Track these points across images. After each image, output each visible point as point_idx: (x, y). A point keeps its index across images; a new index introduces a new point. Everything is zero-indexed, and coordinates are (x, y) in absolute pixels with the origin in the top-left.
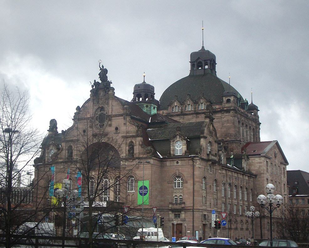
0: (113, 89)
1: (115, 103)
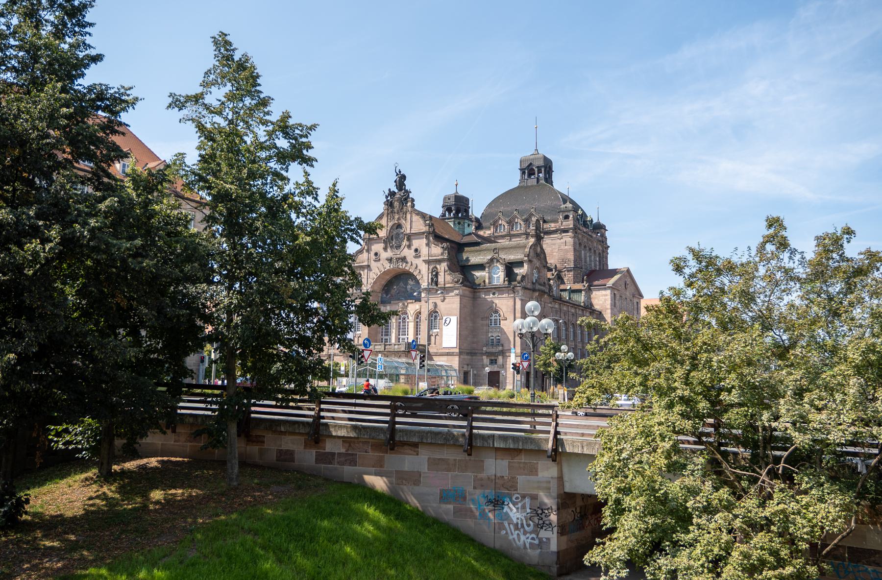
0: (413, 200)
1: (415, 218)
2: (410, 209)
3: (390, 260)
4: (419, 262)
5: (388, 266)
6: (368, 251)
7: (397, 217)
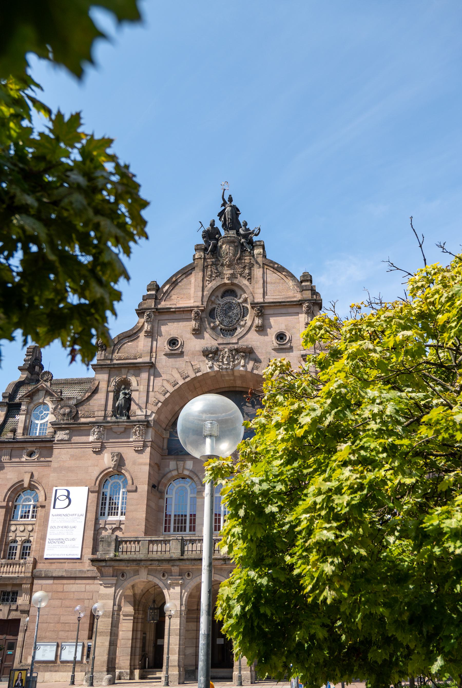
2: (260, 260)
3: (211, 354)
6: (152, 335)
7: (227, 272)
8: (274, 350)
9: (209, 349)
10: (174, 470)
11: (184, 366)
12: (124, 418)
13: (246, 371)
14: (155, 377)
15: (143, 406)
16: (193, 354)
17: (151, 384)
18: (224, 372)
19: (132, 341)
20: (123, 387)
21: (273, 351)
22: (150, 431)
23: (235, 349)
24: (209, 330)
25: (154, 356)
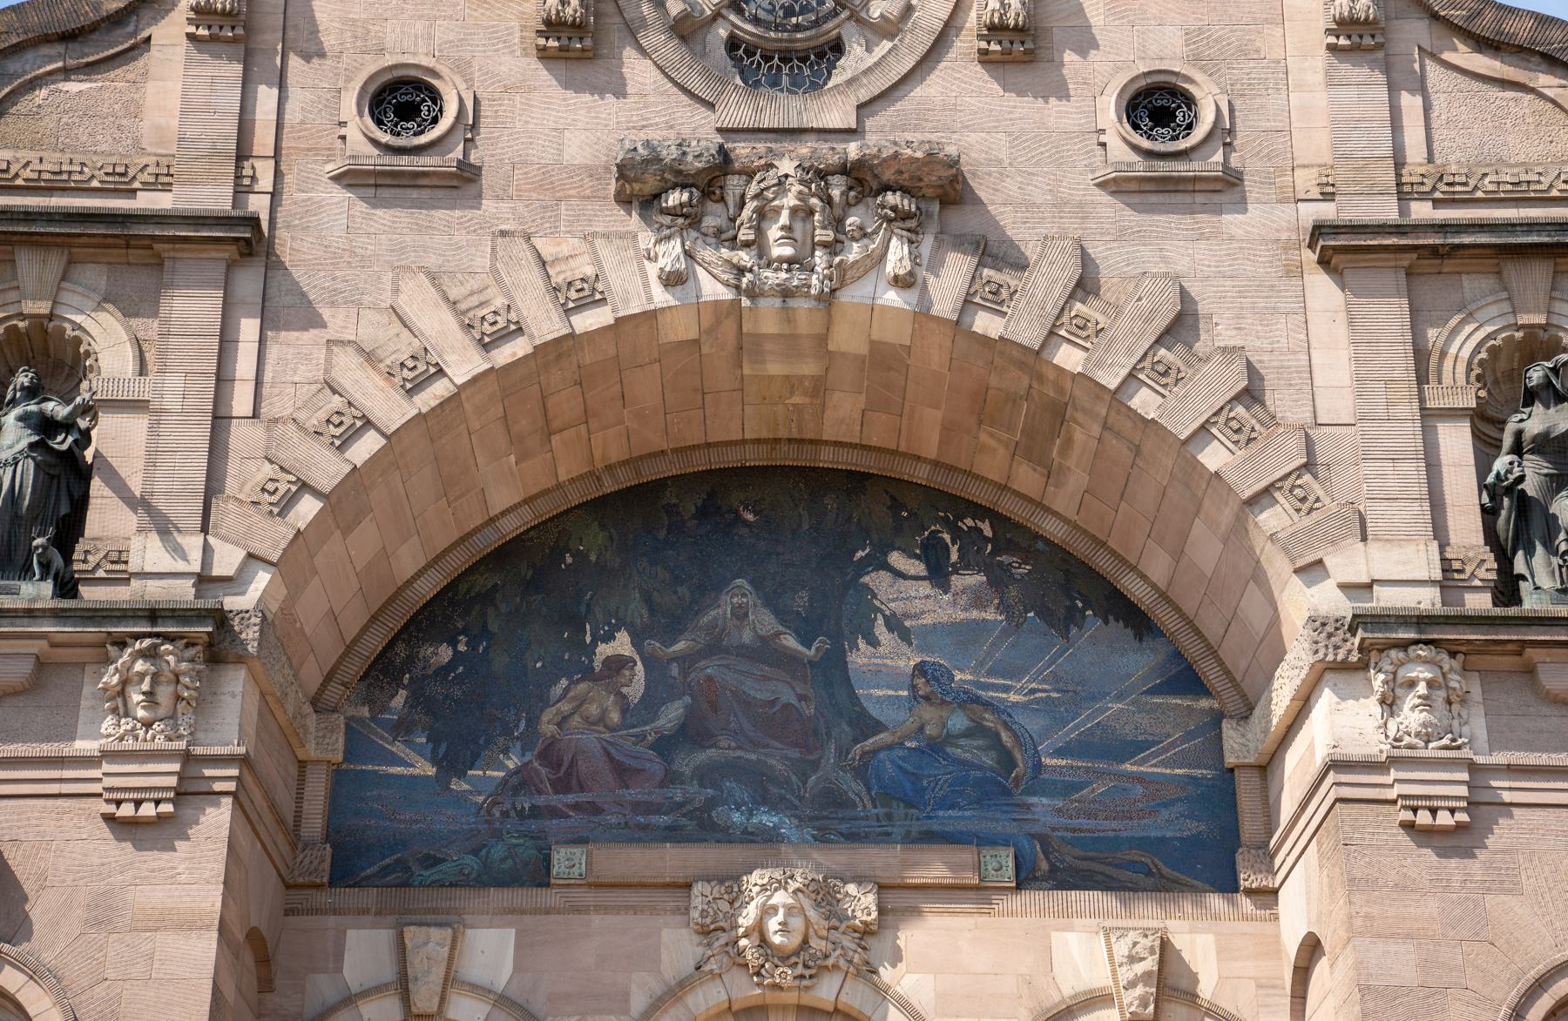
3: (677, 191)
4: (1241, 270)
5: (638, 271)
8: (1116, 186)
9: (670, 154)
10: (378, 989)
11: (482, 261)
12: (37, 591)
13: (923, 315)
14: (269, 322)
15: (186, 511)
16: (551, 187)
17: (245, 365)
18: (767, 318)
19: (91, 69)
20: (23, 379)
21: (1104, 198)
22: (236, 685)
23: (845, 169)
24: (655, 38)
25: (266, 182)
